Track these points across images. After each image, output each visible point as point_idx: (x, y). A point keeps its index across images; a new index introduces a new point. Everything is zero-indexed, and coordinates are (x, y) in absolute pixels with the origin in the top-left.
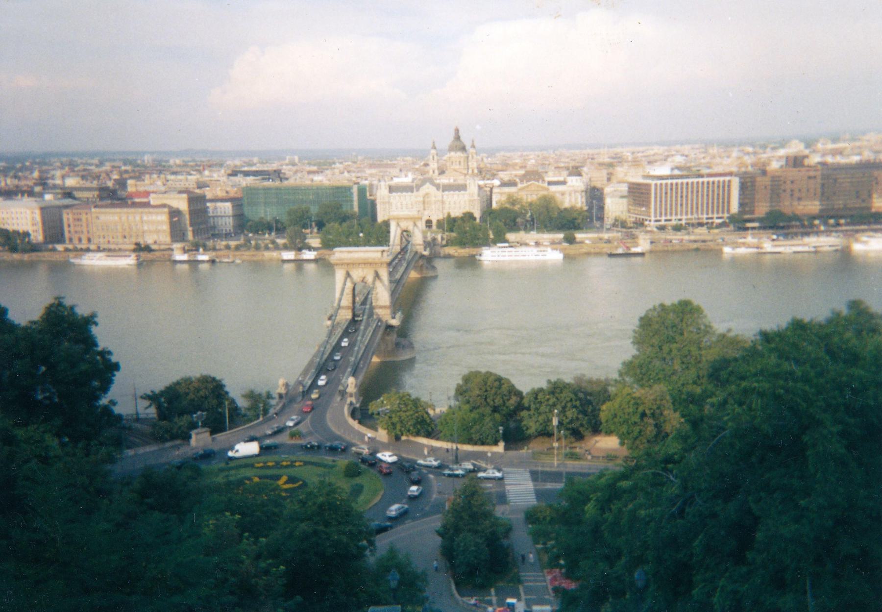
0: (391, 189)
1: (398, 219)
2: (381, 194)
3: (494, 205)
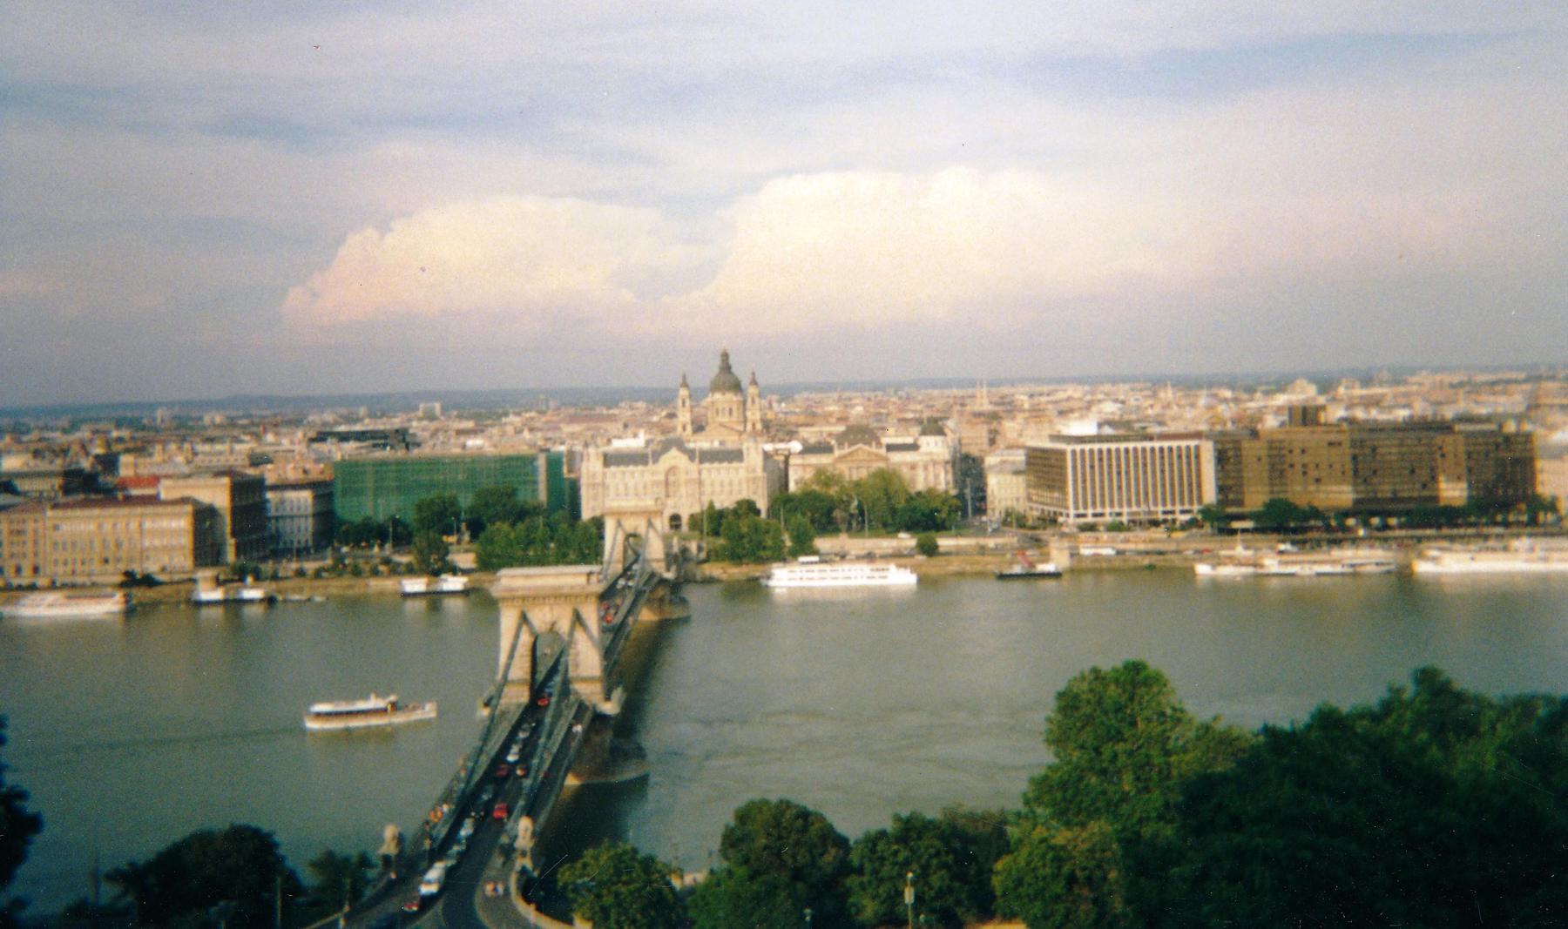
0: (609, 460)
1: (619, 515)
2: (590, 469)
3: (792, 487)
